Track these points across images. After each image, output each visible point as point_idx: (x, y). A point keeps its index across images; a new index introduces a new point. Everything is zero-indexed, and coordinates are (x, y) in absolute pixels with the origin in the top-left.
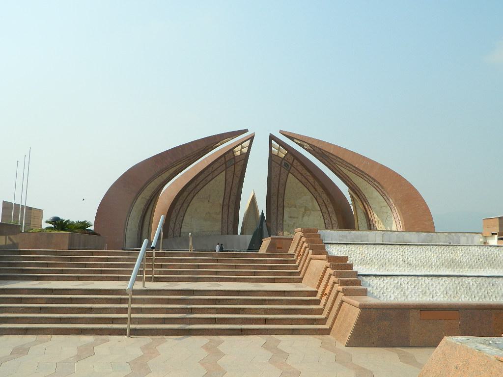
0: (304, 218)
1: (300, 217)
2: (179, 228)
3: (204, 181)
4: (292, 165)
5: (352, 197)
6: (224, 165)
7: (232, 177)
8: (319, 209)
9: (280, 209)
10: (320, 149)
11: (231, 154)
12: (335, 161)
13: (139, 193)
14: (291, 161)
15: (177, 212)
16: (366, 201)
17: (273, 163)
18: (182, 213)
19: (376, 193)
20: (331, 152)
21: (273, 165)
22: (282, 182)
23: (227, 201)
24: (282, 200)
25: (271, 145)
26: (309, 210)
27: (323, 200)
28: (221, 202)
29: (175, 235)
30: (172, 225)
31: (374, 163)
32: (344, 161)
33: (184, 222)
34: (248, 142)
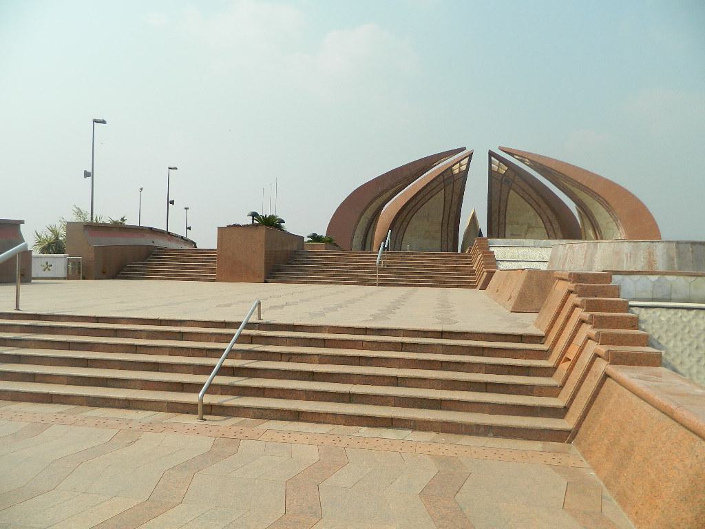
1: (523, 234)
5: (579, 213)
6: (443, 184)
9: (502, 226)
10: (541, 165)
11: (449, 172)
13: (362, 214)
16: (593, 217)
17: (494, 179)
19: (602, 210)
25: (490, 162)
26: (532, 227)
27: (548, 217)
28: (441, 219)
31: (599, 178)
32: (566, 176)
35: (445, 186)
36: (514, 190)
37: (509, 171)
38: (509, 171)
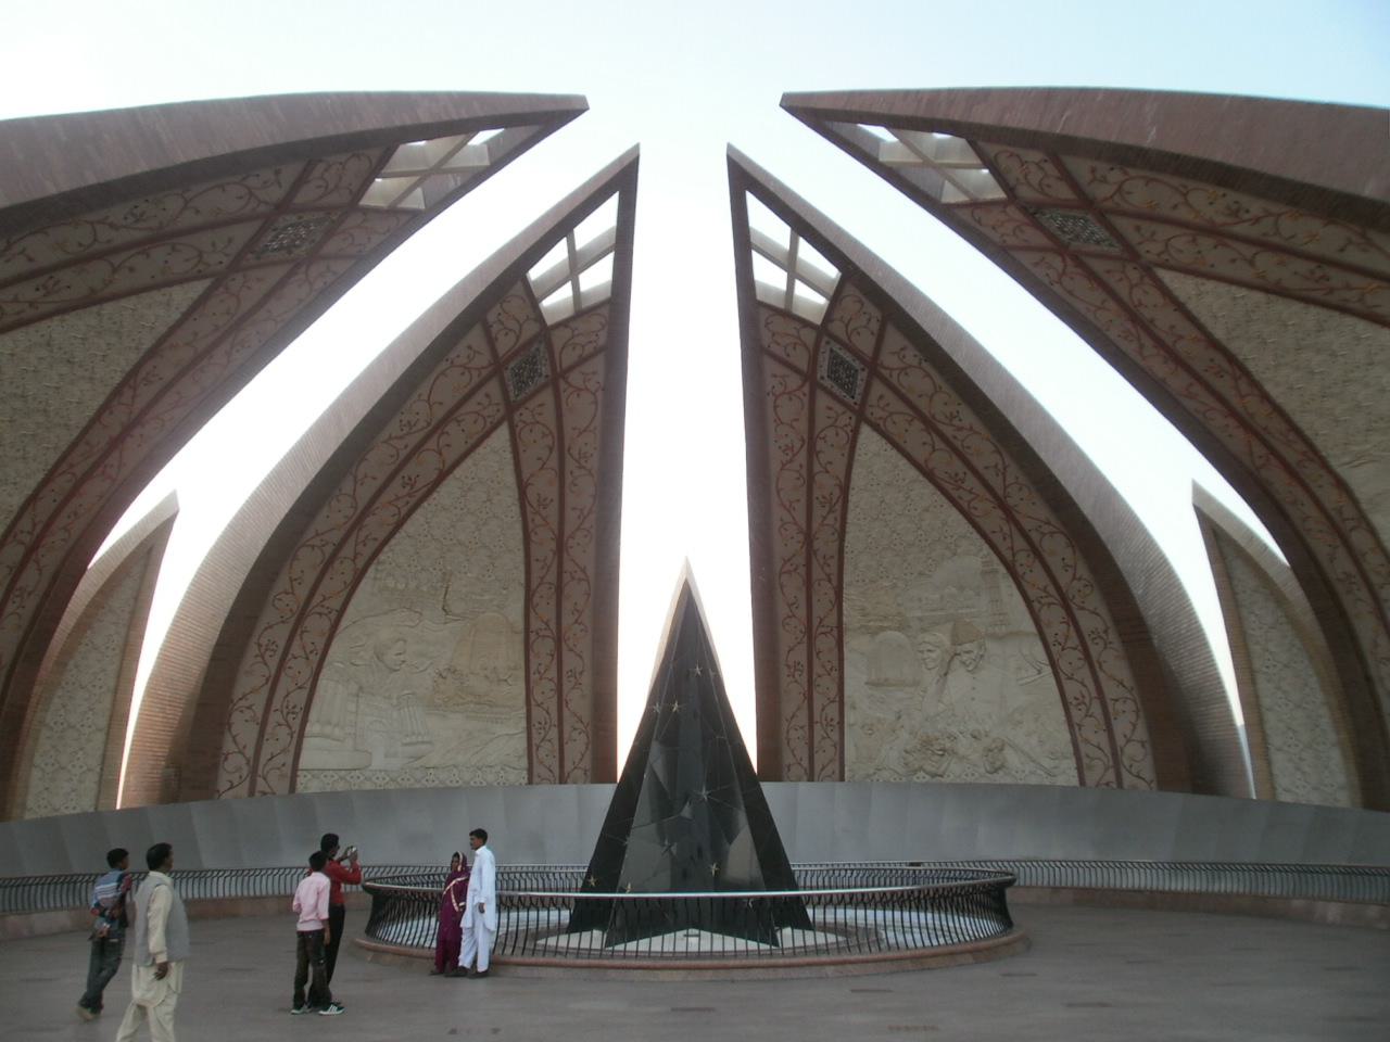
0: (949, 677)
2: (284, 751)
3: (398, 481)
4: (873, 366)
6: (493, 387)
7: (553, 463)
8: (1028, 625)
9: (825, 643)
10: (1058, 148)
14: (865, 344)
15: (273, 663)
18: (299, 668)
20: (1150, 139)
22: (826, 484)
23: (546, 610)
24: (832, 595)
28: (515, 611)
29: (261, 785)
30: (243, 729)
33: (313, 715)
34: (604, 219)
35: (511, 409)
36: (876, 428)
37: (849, 304)
38: (850, 289)
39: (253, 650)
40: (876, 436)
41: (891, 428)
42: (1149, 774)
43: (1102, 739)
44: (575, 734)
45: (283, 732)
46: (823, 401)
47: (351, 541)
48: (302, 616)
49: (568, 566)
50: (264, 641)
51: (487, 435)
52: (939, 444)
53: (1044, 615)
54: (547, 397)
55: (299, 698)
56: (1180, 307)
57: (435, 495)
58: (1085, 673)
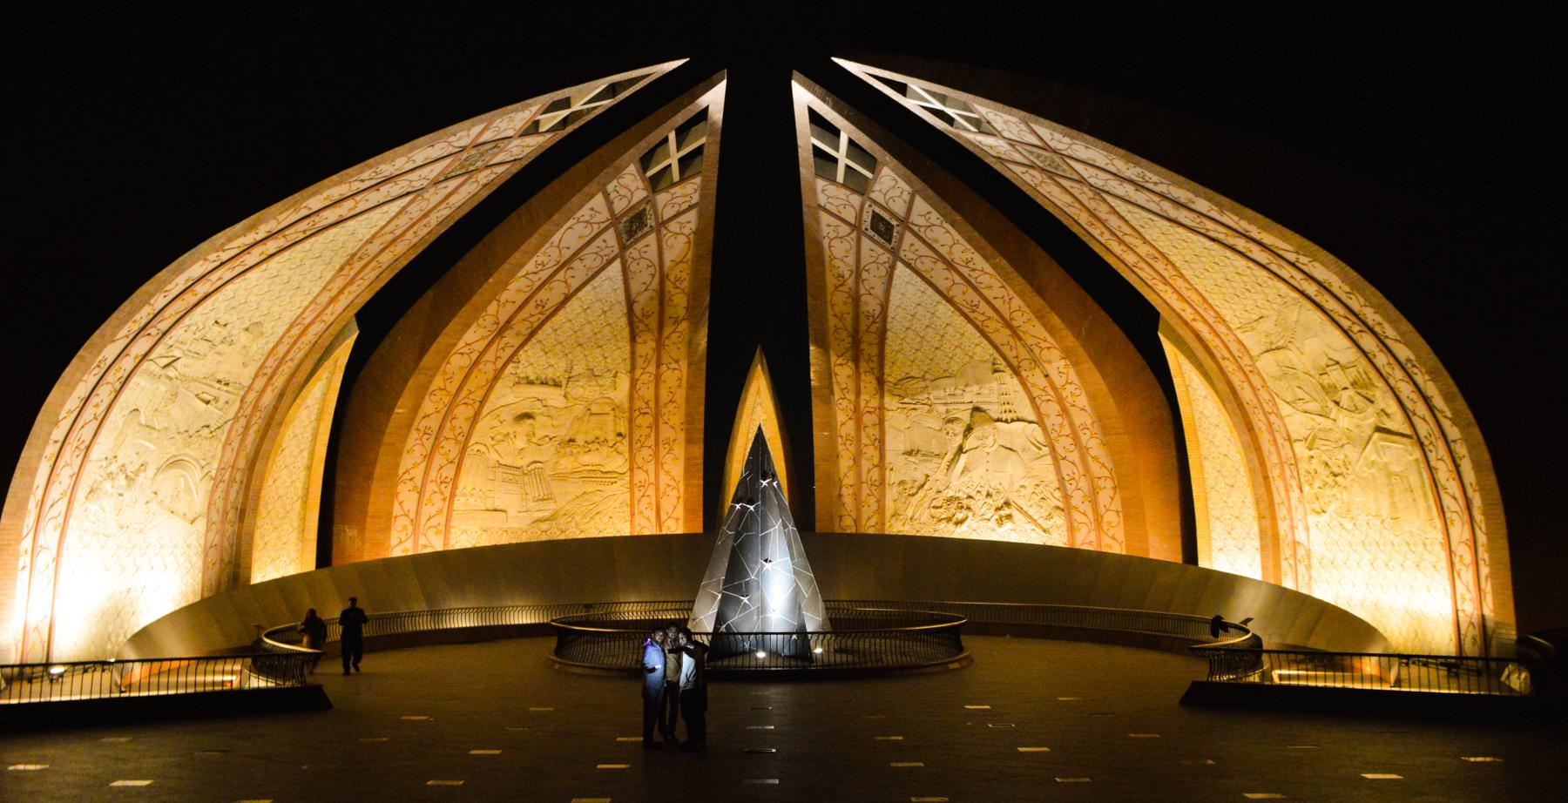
2: (440, 512)
3: (532, 303)
4: (905, 222)
6: (610, 236)
12: (1098, 179)
14: (899, 208)
15: (429, 444)
18: (450, 448)
21: (825, 230)
24: (875, 382)
35: (623, 248)
36: (908, 265)
39: (414, 435)
40: (908, 271)
41: (920, 266)
42: (1121, 536)
43: (1087, 507)
44: (669, 490)
45: (437, 498)
46: (866, 244)
47: (494, 347)
48: (450, 407)
49: (665, 359)
50: (422, 428)
51: (603, 269)
52: (958, 279)
53: (1044, 408)
54: (652, 238)
55: (449, 472)
56: (1122, 218)
57: (561, 313)
58: (1075, 456)
